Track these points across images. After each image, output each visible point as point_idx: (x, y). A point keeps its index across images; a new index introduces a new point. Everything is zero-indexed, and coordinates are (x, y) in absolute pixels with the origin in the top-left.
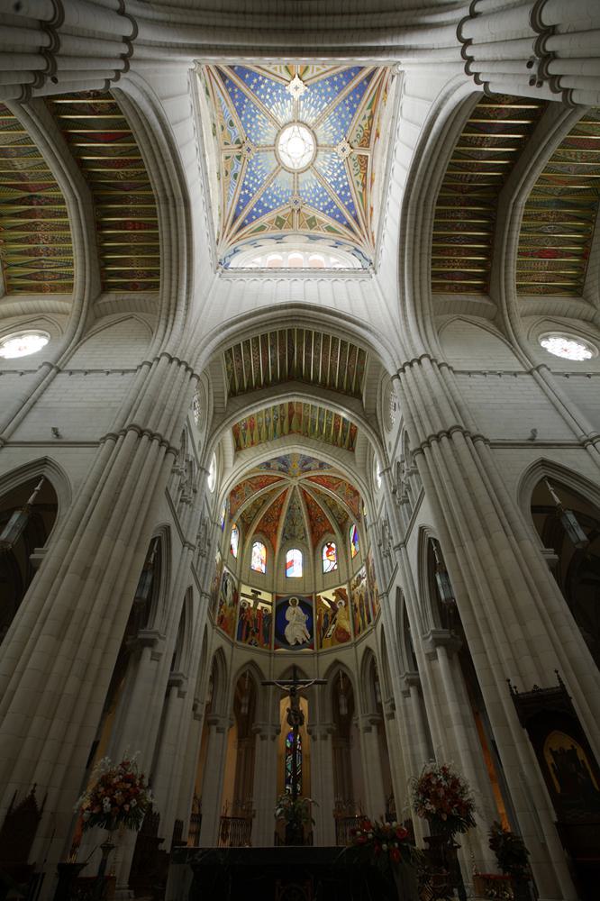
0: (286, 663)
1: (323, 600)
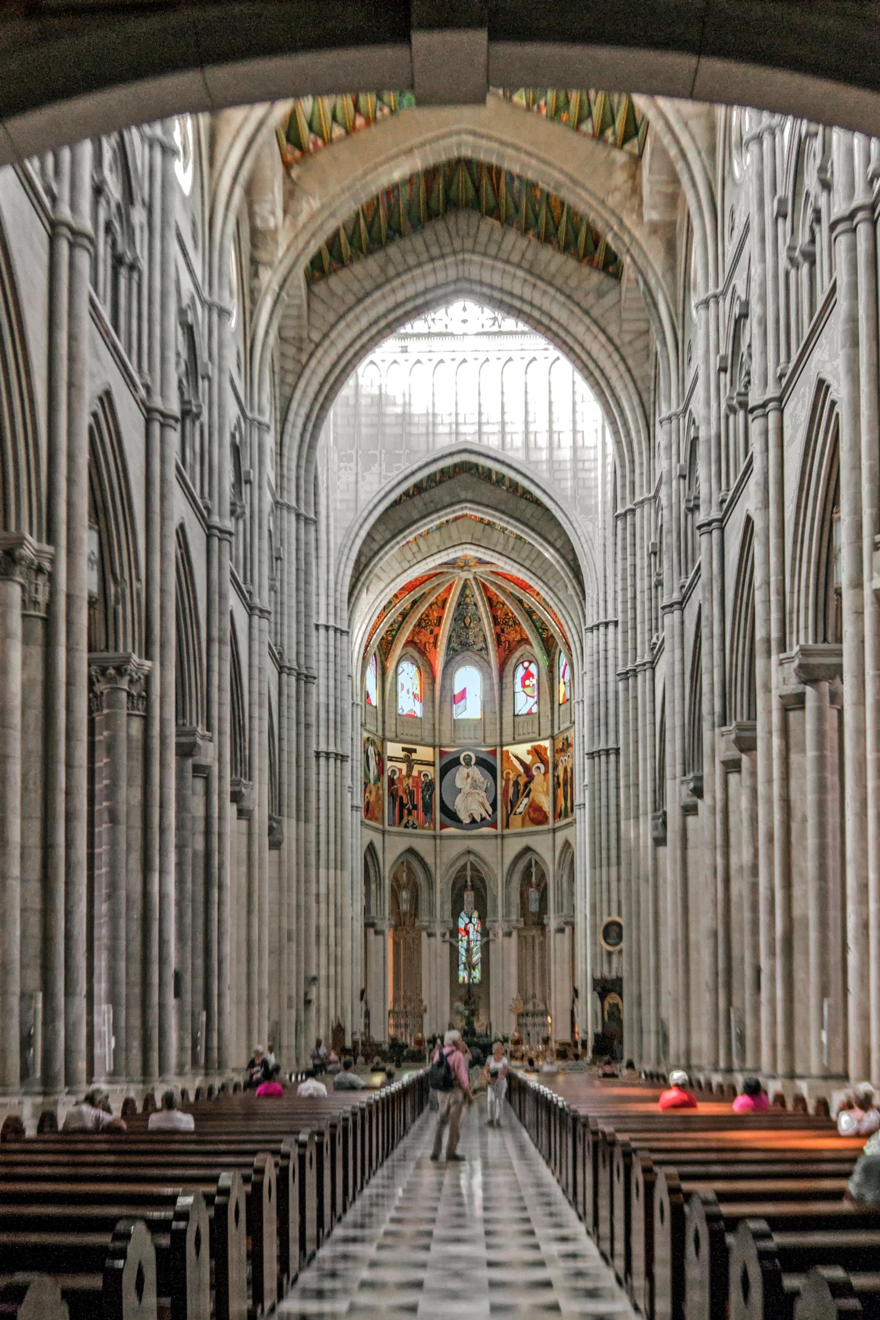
0: (457, 847)
1: (513, 758)
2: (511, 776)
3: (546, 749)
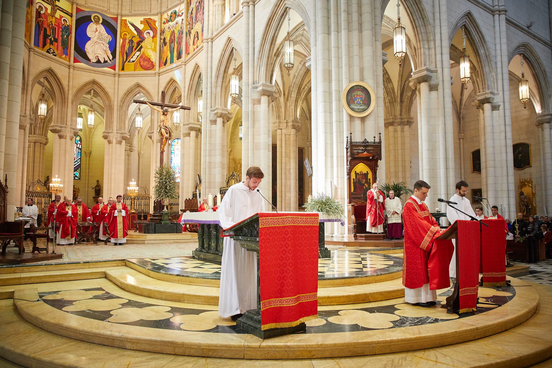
1: (129, 25)
2: (128, 37)
3: (155, 21)
